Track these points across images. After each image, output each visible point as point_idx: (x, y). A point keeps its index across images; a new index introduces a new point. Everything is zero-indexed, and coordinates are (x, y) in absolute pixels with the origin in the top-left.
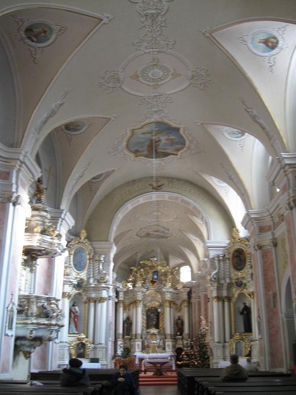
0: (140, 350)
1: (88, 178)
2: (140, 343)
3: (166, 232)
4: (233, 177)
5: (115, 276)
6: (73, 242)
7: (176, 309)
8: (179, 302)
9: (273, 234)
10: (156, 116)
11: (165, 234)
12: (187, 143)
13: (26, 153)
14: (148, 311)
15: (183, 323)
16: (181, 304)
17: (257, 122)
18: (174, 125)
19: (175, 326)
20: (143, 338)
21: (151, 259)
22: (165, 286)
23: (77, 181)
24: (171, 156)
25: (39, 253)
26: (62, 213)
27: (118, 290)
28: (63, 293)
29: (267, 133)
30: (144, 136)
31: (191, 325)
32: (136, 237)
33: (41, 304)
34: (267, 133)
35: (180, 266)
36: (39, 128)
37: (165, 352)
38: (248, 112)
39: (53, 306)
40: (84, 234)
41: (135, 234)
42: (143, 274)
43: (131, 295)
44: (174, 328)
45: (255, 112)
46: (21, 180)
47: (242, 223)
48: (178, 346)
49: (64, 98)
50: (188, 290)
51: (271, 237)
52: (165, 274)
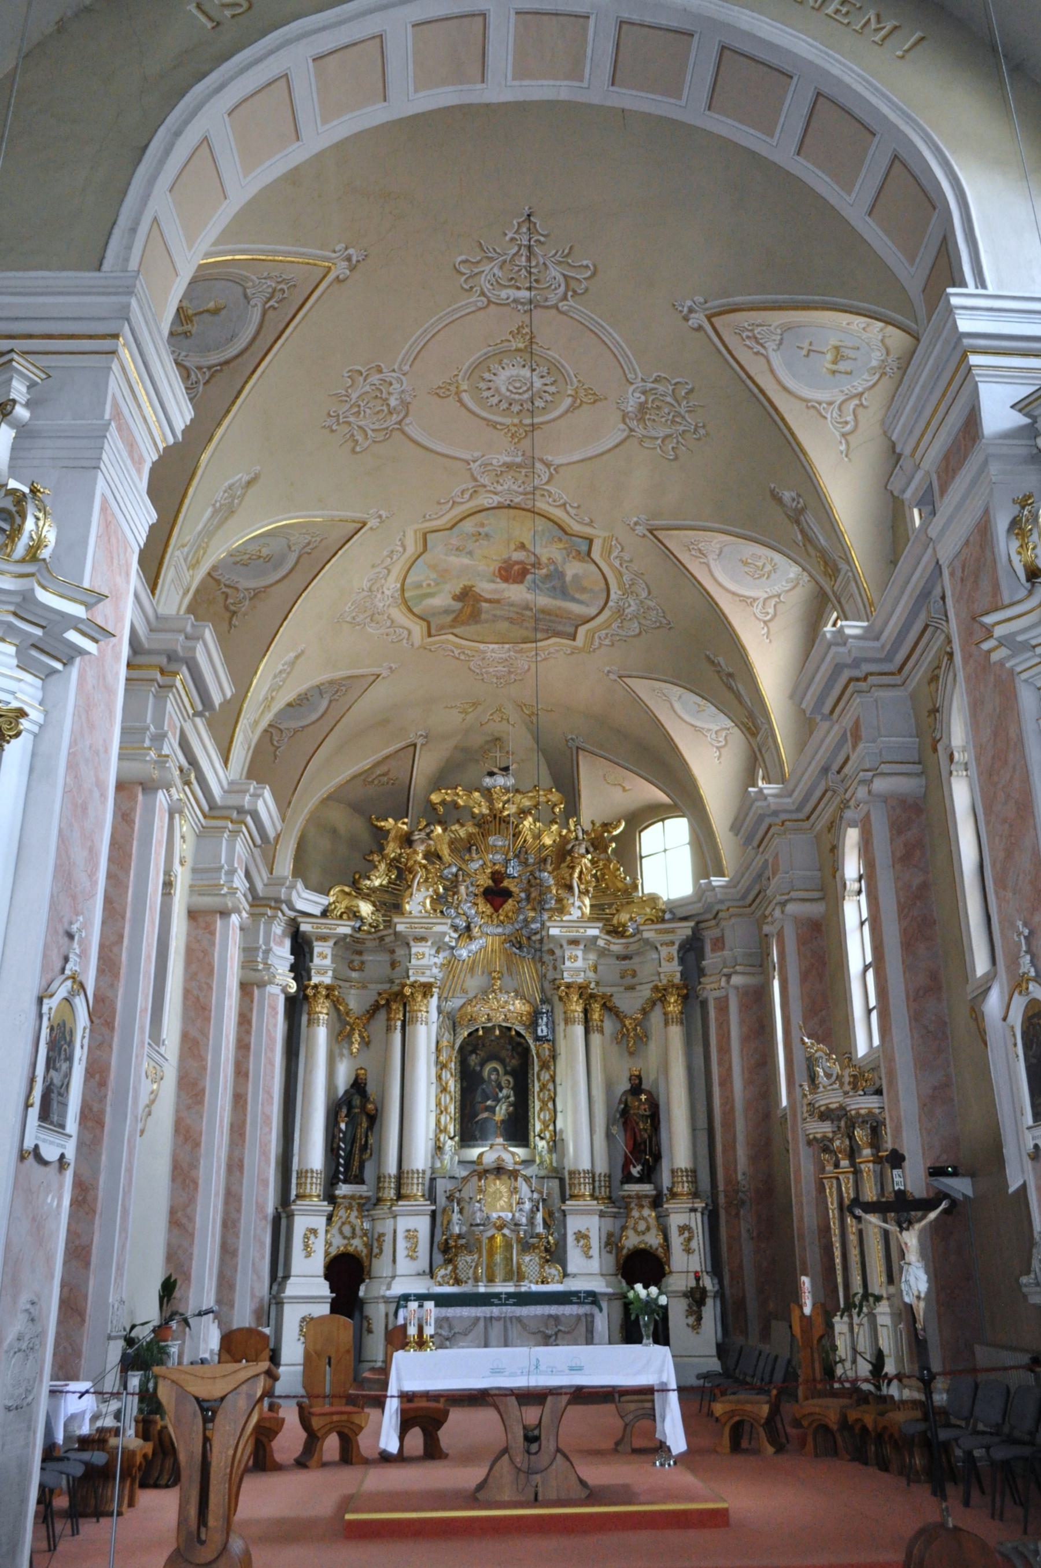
0: (423, 1263)
2: (422, 1225)
3: (573, 569)
7: (621, 1037)
8: (629, 1003)
14: (465, 1051)
15: (654, 1115)
16: (645, 1012)
19: (615, 1130)
20: (441, 1200)
21: (488, 781)
22: (562, 910)
27: (304, 927)
31: (702, 1123)
37: (565, 1275)
41: (392, 585)
42: (445, 852)
43: (375, 961)
44: (609, 1136)
48: (631, 1241)
50: (684, 930)
52: (563, 853)
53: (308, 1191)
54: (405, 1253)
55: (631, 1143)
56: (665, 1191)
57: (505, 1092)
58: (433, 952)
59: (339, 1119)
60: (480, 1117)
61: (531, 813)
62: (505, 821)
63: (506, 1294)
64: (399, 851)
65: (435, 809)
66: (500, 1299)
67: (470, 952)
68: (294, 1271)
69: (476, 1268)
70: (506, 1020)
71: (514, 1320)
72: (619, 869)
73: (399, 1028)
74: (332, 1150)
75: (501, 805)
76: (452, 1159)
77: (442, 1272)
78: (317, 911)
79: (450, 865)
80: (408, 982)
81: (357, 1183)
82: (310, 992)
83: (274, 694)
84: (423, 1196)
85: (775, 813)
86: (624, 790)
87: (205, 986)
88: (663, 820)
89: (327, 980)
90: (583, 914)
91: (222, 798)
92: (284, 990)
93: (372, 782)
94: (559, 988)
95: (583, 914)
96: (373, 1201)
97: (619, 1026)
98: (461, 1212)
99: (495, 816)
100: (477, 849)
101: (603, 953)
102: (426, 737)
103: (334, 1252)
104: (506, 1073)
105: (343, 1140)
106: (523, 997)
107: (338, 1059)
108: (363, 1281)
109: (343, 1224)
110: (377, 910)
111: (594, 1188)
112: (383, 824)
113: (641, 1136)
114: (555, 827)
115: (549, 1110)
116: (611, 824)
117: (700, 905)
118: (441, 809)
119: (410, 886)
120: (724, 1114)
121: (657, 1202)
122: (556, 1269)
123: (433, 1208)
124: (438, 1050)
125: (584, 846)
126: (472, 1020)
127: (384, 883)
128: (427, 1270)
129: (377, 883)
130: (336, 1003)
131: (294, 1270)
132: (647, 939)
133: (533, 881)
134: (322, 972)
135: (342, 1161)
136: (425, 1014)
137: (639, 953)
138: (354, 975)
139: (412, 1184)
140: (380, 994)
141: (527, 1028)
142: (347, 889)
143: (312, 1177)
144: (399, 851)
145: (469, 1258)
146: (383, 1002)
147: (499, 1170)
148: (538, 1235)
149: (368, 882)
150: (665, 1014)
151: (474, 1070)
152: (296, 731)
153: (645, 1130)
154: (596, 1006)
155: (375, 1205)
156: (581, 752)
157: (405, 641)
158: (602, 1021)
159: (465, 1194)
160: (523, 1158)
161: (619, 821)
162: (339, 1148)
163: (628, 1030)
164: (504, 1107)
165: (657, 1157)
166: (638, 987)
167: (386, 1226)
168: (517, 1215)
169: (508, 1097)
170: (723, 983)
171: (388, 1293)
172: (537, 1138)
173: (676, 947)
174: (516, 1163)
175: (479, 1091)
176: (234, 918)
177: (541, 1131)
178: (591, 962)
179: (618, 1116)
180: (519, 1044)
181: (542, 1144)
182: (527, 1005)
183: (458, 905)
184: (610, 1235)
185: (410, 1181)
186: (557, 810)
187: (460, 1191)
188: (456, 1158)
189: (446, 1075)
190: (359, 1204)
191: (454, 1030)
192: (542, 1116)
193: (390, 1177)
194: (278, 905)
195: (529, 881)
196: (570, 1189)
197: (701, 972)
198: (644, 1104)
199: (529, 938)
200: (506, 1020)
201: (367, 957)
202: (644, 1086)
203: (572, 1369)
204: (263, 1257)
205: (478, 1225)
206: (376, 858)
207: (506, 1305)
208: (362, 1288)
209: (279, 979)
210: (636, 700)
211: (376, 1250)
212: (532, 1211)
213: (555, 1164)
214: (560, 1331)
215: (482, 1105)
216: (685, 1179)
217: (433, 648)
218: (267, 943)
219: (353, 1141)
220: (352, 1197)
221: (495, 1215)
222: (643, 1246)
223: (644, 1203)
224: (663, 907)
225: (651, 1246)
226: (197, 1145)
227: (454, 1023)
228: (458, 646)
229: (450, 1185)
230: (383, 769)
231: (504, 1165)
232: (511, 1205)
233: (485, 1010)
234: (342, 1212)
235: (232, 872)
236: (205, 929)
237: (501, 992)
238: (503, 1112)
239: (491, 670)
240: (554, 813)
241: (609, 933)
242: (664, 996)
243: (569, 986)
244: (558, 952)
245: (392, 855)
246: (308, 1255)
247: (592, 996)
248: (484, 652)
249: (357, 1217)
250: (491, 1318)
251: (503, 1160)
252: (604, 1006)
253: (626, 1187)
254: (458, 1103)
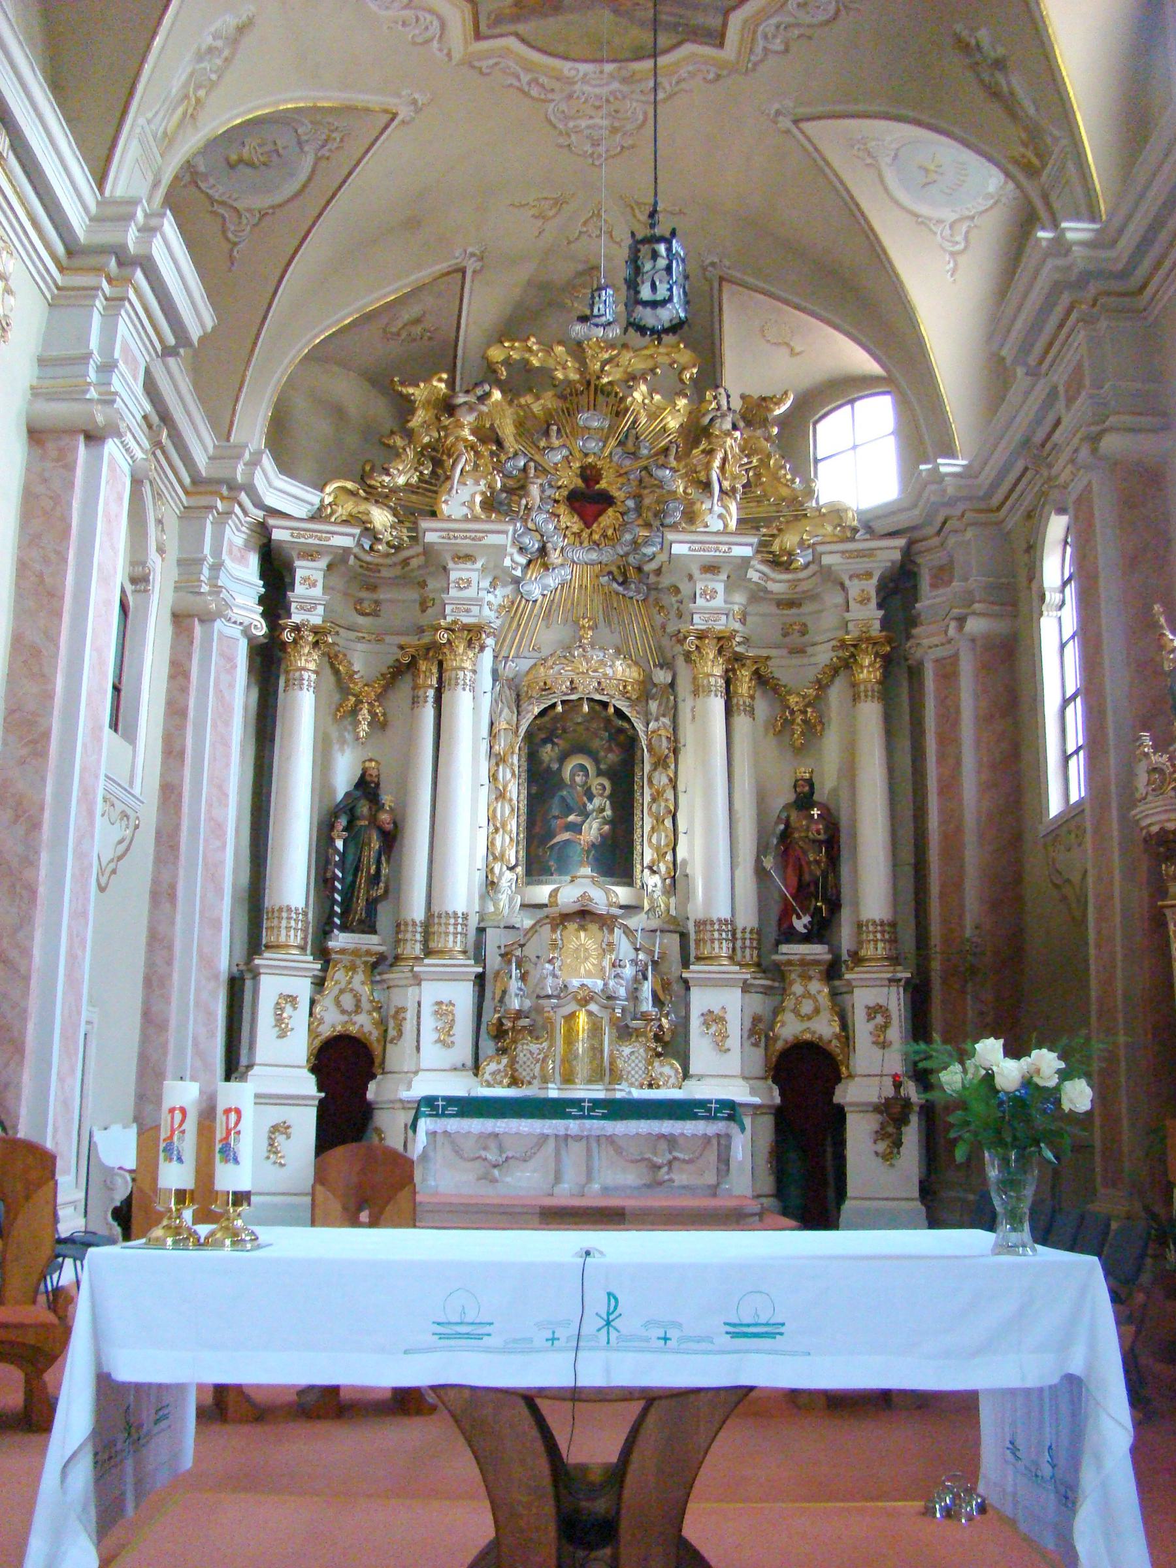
0: (463, 1050)
2: (462, 995)
7: (782, 726)
14: (534, 741)
16: (822, 686)
19: (769, 863)
20: (493, 961)
21: (579, 330)
27: (277, 535)
31: (908, 856)
37: (686, 1075)
44: (761, 873)
48: (790, 1029)
50: (890, 552)
53: (283, 939)
54: (435, 1036)
55: (793, 880)
56: (845, 957)
57: (597, 801)
58: (485, 584)
59: (335, 834)
60: (555, 841)
61: (645, 380)
63: (590, 1101)
64: (436, 435)
65: (495, 372)
66: (582, 1109)
67: (545, 587)
69: (544, 1060)
70: (600, 689)
71: (603, 1140)
72: (784, 467)
73: (431, 700)
74: (326, 881)
75: (598, 366)
76: (511, 900)
77: (493, 1066)
78: (300, 511)
79: (516, 454)
80: (443, 623)
81: (363, 932)
82: (287, 636)
83: (202, 93)
84: (464, 952)
85: (1084, 279)
86: (793, 353)
87: (53, 557)
88: (852, 402)
89: (316, 619)
90: (726, 526)
91: (89, 231)
92: (246, 632)
93: (398, 334)
94: (686, 638)
95: (726, 526)
96: (390, 960)
97: (778, 710)
98: (523, 978)
99: (589, 383)
100: (559, 431)
101: (758, 595)
102: (481, 259)
103: (326, 1031)
104: (600, 773)
105: (342, 865)
106: (628, 656)
107: (336, 747)
108: (373, 1076)
109: (342, 991)
110: (400, 522)
111: (734, 949)
112: (411, 390)
113: (811, 872)
114: (682, 403)
115: (666, 829)
116: (771, 399)
117: (916, 512)
118: (503, 373)
119: (448, 478)
120: (945, 837)
121: (832, 971)
122: (672, 1066)
123: (480, 970)
124: (493, 734)
125: (729, 419)
126: (546, 689)
127: (414, 480)
128: (469, 1062)
129: (401, 480)
130: (332, 660)
131: (260, 1057)
132: (829, 567)
133: (647, 479)
134: (309, 608)
135: (338, 897)
136: (469, 675)
137: (813, 597)
138: (361, 620)
139: (447, 934)
140: (401, 647)
141: (633, 703)
142: (350, 485)
143: (289, 918)
144: (436, 435)
145: (534, 1047)
146: (406, 660)
147: (584, 915)
148: (644, 1016)
149: (387, 479)
150: (854, 685)
151: (549, 768)
152: (263, 215)
153: (817, 862)
154: (745, 674)
155: (391, 965)
156: (724, 283)
157: (435, 44)
158: (752, 697)
159: (530, 951)
160: (623, 902)
161: (786, 393)
162: (335, 877)
163: (792, 712)
164: (595, 825)
165: (835, 906)
166: (810, 650)
167: (407, 997)
168: (611, 983)
169: (603, 810)
170: (952, 632)
171: (405, 1094)
172: (646, 872)
173: (874, 581)
174: (610, 905)
175: (556, 800)
176: (111, 447)
177: (653, 861)
178: (736, 608)
179: (775, 841)
180: (621, 731)
181: (653, 881)
182: (634, 669)
183: (528, 515)
184: (756, 1020)
185: (443, 929)
186: (687, 375)
187: (522, 946)
188: (518, 900)
189: (504, 773)
190: (365, 963)
191: (518, 706)
192: (654, 841)
193: (414, 924)
194: (233, 494)
195: (641, 481)
196: (697, 948)
197: (913, 621)
198: (817, 822)
199: (639, 569)
200: (600, 689)
201: (382, 595)
202: (816, 798)
203: (738, 1331)
204: (212, 1035)
205: (549, 997)
206: (399, 441)
207: (590, 1117)
208: (372, 1086)
209: (237, 614)
210: (819, 166)
211: (392, 1033)
212: (635, 980)
213: (673, 912)
214: (675, 1158)
215: (559, 822)
216: (879, 936)
217: (484, 64)
218: (217, 551)
219: (357, 869)
220: (356, 953)
221: (575, 982)
222: (807, 1036)
223: (811, 973)
224: (855, 523)
225: (820, 1038)
226: (35, 825)
227: (518, 695)
228: (528, 67)
229: (508, 938)
230: (414, 311)
231: (592, 907)
232: (603, 969)
233: (567, 672)
235: (108, 367)
236: (58, 460)
237: (593, 647)
238: (594, 832)
239: (583, 123)
240: (682, 381)
241: (765, 562)
242: (853, 656)
243: (701, 636)
244: (685, 588)
245: (426, 439)
246: (282, 1035)
247: (738, 658)
248: (570, 82)
249: (363, 983)
250: (567, 1137)
251: (591, 900)
252: (757, 676)
253: (784, 948)
254: (523, 818)
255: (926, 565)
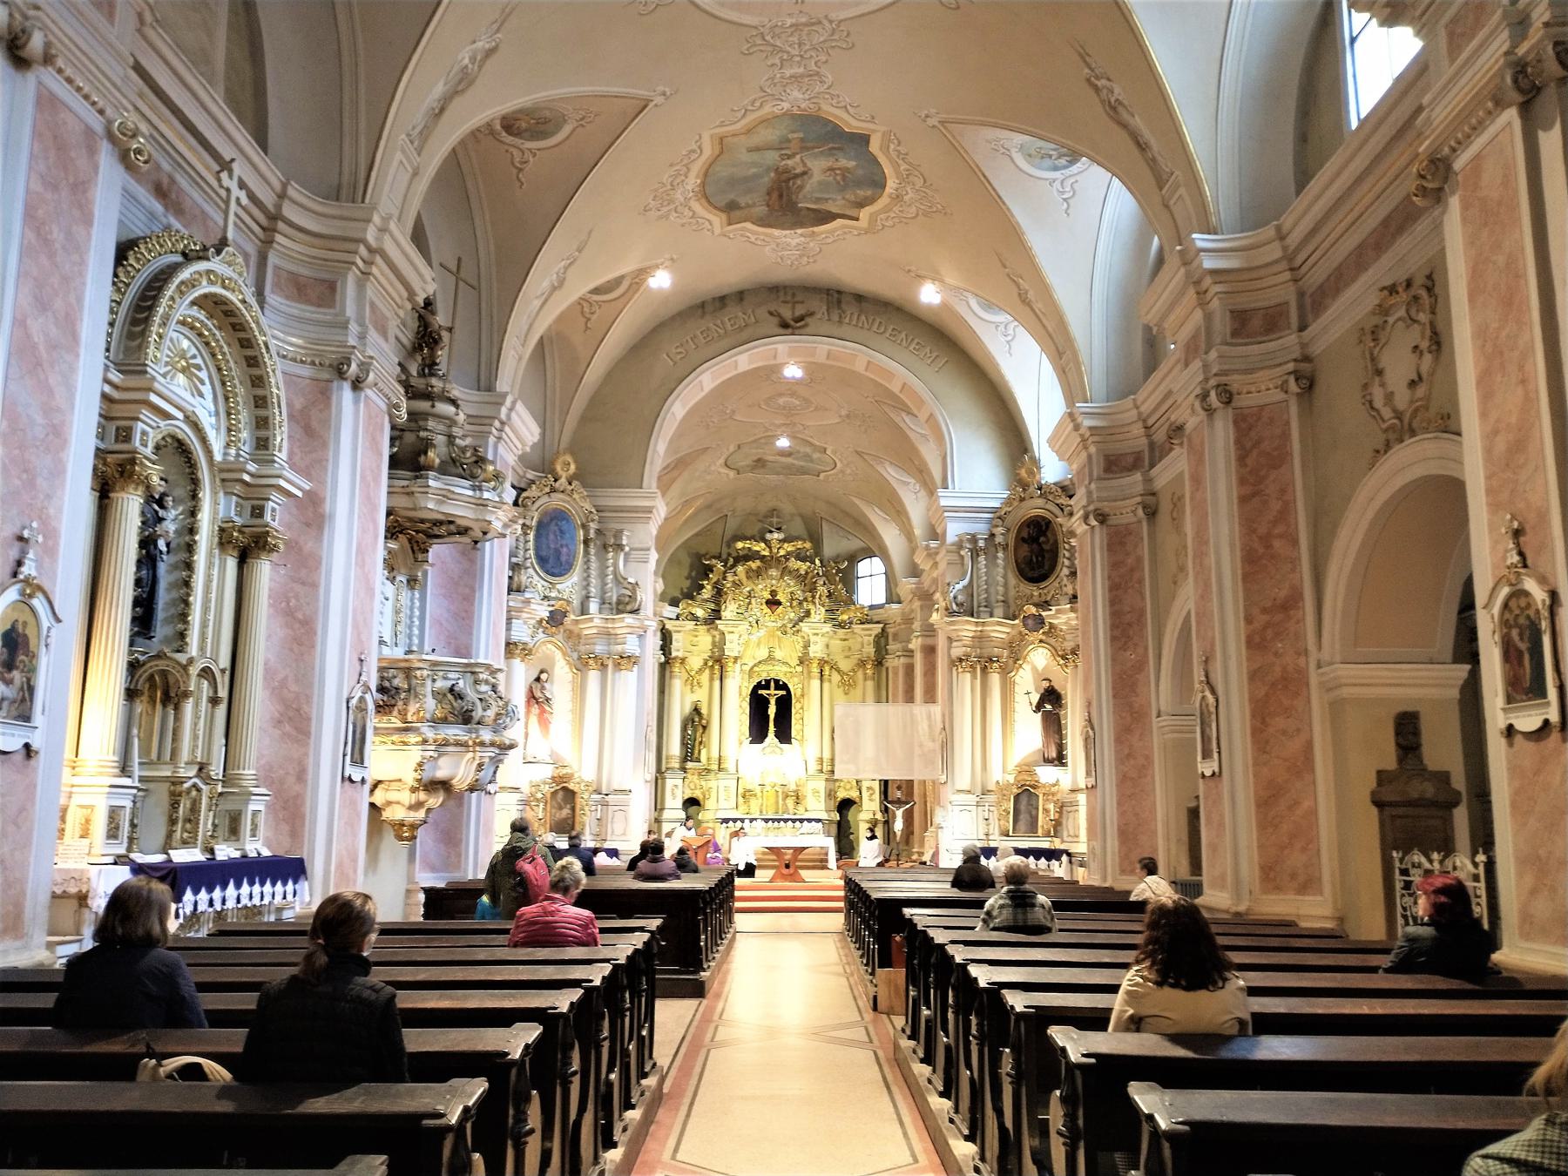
1: (577, 289)
3: (816, 456)
4: (1031, 295)
5: (660, 587)
6: (533, 492)
7: (843, 683)
8: (845, 665)
9: (1148, 480)
10: (796, 94)
11: (812, 461)
12: (891, 185)
13: (386, 219)
17: (1124, 126)
18: (852, 124)
21: (768, 536)
23: (546, 300)
24: (839, 222)
25: (436, 531)
26: (501, 404)
28: (508, 644)
29: (1152, 163)
30: (755, 156)
32: (724, 470)
33: (449, 684)
34: (1152, 163)
35: (853, 559)
36: (421, 133)
38: (1097, 89)
39: (484, 688)
40: (566, 467)
41: (722, 461)
45: (1117, 91)
46: (372, 304)
47: (1051, 441)
49: (498, 31)
51: (1140, 488)
62: (778, 560)
68: (667, 806)
234: (689, 776)
247: (826, 662)
255: (891, 631)
